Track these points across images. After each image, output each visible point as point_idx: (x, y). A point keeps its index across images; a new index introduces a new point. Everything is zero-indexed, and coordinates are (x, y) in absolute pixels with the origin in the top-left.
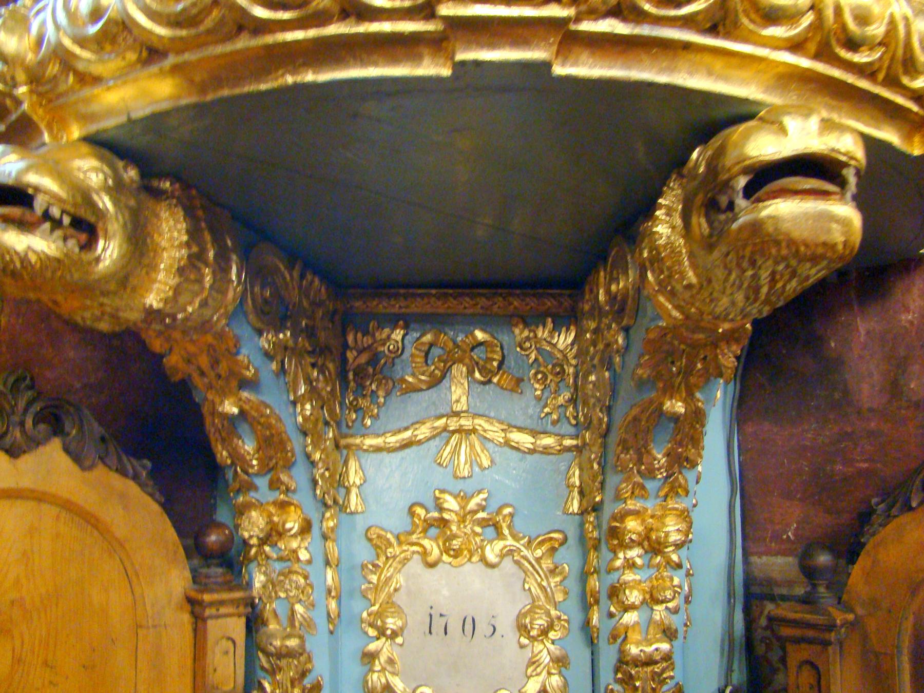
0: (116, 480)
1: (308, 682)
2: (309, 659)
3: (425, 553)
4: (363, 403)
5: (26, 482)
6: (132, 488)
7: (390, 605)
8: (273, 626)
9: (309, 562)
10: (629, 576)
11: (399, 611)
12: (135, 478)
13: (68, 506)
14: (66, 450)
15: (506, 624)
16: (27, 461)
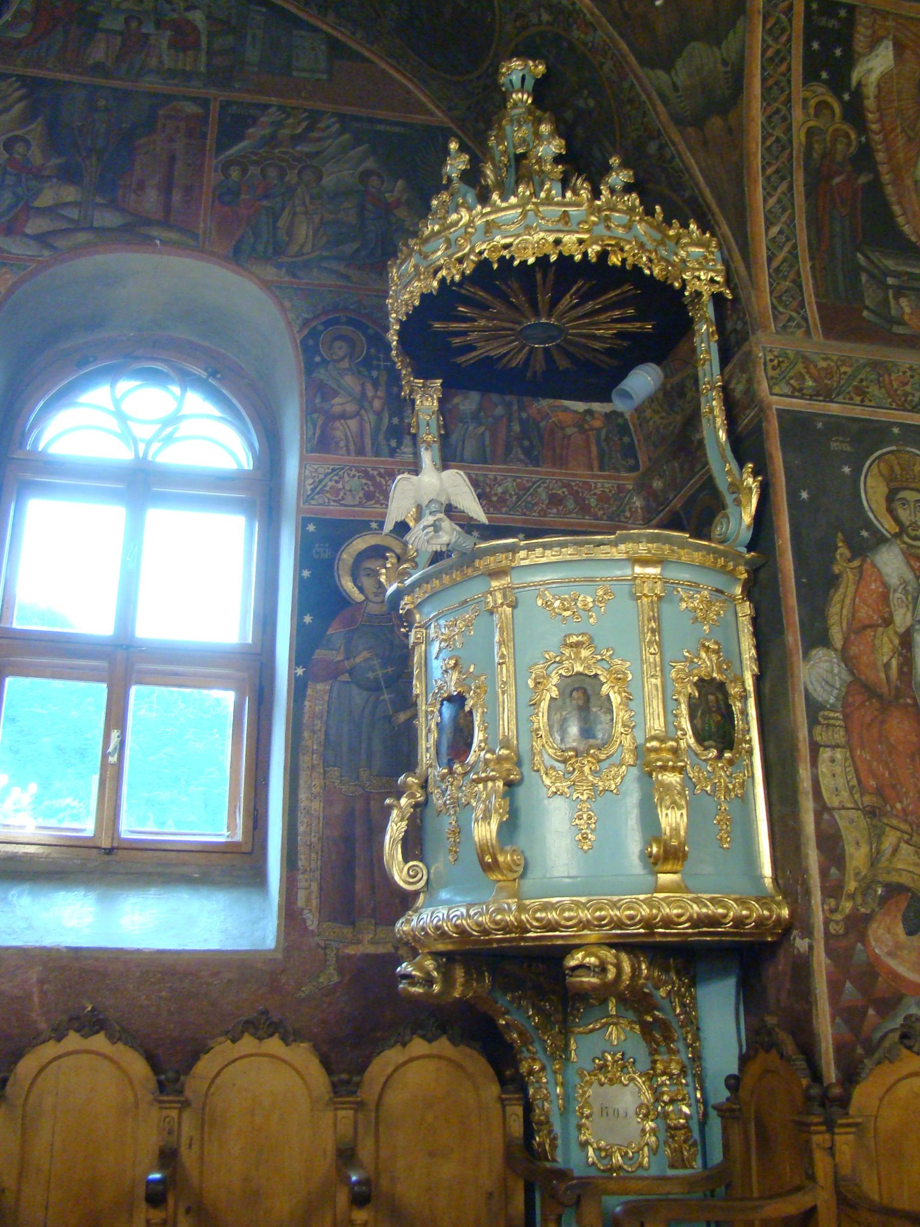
0: (468, 1050)
1: (552, 1136)
2: (551, 1126)
3: (599, 1080)
4: (575, 1012)
5: (435, 1052)
6: (475, 1054)
7: (587, 1104)
8: (537, 1111)
9: (547, 1083)
10: (665, 1089)
11: (590, 1106)
12: (475, 1049)
13: (450, 1060)
14: (449, 1040)
15: (631, 1112)
16: (435, 1044)
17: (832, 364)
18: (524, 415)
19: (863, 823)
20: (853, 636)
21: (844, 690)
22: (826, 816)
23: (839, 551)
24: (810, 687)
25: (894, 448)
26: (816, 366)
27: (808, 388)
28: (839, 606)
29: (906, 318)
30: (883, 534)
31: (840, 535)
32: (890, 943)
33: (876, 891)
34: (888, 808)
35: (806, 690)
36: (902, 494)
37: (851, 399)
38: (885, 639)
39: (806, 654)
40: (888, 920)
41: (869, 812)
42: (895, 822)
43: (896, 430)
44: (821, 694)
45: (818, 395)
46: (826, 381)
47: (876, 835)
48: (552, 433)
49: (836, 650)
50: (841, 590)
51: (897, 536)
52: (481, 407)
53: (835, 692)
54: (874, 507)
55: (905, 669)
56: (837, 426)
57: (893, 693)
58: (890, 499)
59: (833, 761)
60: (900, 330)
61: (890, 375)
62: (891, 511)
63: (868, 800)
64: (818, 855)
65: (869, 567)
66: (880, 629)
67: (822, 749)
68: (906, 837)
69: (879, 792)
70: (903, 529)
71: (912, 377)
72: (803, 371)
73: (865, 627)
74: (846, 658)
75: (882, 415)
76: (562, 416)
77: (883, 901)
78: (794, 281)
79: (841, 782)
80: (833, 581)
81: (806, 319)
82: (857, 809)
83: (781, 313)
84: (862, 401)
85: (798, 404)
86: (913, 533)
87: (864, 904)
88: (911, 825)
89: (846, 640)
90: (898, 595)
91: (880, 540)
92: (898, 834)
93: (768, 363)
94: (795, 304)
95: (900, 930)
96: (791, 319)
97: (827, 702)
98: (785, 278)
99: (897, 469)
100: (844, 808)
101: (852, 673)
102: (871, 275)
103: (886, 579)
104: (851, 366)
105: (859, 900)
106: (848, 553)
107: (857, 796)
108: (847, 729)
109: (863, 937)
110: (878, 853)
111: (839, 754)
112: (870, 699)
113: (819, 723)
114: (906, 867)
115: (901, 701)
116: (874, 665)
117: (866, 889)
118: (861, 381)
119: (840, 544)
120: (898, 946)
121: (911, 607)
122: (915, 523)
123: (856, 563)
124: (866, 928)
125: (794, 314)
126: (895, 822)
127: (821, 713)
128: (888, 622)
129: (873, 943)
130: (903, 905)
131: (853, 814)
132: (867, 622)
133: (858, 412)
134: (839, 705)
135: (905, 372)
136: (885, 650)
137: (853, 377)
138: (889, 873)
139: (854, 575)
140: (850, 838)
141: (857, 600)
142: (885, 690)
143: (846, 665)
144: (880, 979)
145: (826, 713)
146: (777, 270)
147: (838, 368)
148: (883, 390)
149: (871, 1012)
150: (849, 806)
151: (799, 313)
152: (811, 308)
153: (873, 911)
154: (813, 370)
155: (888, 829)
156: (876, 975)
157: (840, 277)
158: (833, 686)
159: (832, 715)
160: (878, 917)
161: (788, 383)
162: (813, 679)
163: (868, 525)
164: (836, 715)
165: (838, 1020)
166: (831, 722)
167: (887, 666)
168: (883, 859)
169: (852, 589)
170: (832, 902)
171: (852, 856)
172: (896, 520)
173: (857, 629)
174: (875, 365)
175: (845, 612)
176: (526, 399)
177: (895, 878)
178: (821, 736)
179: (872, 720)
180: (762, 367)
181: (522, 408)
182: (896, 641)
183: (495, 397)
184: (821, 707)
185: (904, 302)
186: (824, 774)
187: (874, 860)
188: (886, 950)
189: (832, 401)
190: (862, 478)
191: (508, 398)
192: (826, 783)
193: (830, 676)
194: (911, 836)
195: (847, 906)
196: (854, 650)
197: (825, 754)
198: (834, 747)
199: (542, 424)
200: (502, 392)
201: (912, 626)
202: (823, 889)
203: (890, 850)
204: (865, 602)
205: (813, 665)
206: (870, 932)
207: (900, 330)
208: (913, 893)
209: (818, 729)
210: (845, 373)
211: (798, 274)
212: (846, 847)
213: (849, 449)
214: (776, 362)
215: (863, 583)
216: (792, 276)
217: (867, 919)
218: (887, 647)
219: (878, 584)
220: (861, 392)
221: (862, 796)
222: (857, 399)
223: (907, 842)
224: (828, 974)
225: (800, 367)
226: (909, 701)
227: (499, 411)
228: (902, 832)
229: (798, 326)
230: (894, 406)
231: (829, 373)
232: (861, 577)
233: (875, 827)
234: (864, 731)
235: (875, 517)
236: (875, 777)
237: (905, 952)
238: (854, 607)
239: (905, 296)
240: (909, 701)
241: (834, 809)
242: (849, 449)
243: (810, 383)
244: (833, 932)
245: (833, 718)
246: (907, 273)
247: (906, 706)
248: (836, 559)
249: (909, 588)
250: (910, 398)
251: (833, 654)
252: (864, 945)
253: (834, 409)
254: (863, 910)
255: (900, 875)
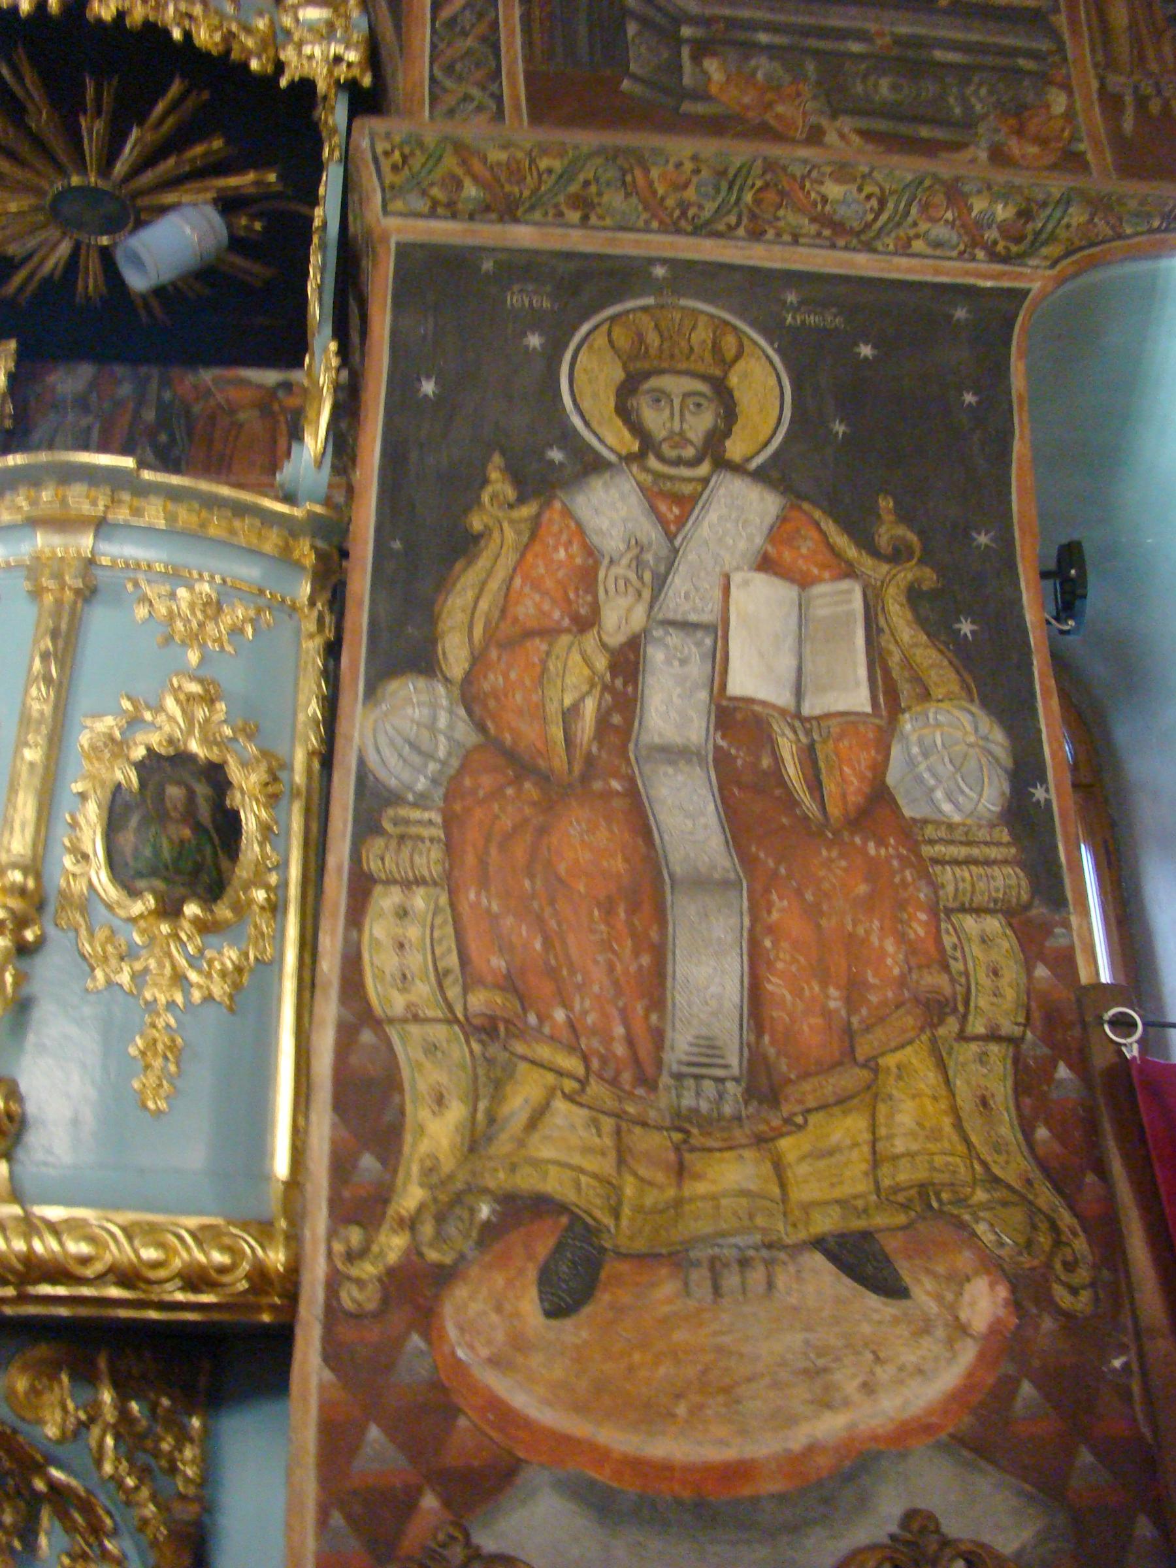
17: (520, 155)
18: (167, 396)
19: (459, 1050)
20: (494, 654)
21: (455, 763)
22: (367, 1036)
23: (489, 489)
24: (372, 759)
25: (650, 301)
26: (484, 159)
27: (468, 199)
28: (470, 595)
29: (714, 89)
30: (597, 456)
31: (497, 459)
32: (500, 1336)
33: (473, 1211)
34: (532, 1019)
35: (361, 762)
36: (654, 382)
37: (560, 214)
38: (575, 657)
39: (371, 691)
40: (499, 1280)
41: (479, 1029)
42: (544, 1052)
43: (660, 271)
44: (393, 769)
45: (488, 209)
46: (508, 188)
47: (491, 1082)
48: (212, 419)
49: (447, 680)
50: (483, 562)
51: (638, 458)
52: (93, 385)
53: (432, 767)
54: (585, 405)
55: (616, 719)
56: (523, 267)
57: (577, 769)
58: (627, 390)
59: (403, 913)
60: (700, 108)
61: (647, 171)
62: (624, 411)
63: (479, 1001)
64: (334, 1126)
65: (556, 516)
66: (565, 639)
67: (378, 889)
68: (569, 1085)
69: (510, 984)
70: (648, 444)
71: (697, 171)
72: (459, 172)
73: (529, 634)
74: (470, 696)
75: (629, 245)
76: (233, 394)
77: (489, 1233)
78: (483, 39)
79: (415, 960)
80: (464, 545)
81: (499, 99)
82: (452, 1020)
83: (445, 90)
84: (585, 218)
85: (445, 231)
86: (672, 454)
87: (440, 1237)
88: (585, 1059)
89: (478, 660)
90: (619, 570)
91: (591, 465)
92: (550, 1078)
93: (382, 159)
94: (479, 75)
95: (529, 1305)
96: (467, 98)
97: (410, 788)
98: (465, 34)
99: (653, 339)
100: (416, 1018)
101: (481, 728)
102: (644, 21)
103: (595, 539)
104: (561, 155)
105: (427, 1229)
106: (511, 493)
107: (453, 992)
108: (450, 848)
109: (426, 1319)
110: (491, 1120)
111: (419, 901)
112: (517, 781)
113: (379, 831)
114: (563, 1157)
115: (597, 785)
116: (539, 713)
117: (449, 1204)
118: (587, 184)
119: (494, 475)
120: (519, 1343)
121: (647, 594)
122: (682, 433)
123: (527, 511)
124: (437, 1298)
125: (475, 92)
126: (544, 1052)
127: (391, 812)
128: (586, 622)
129: (452, 1332)
130: (543, 1248)
131: (439, 1033)
132: (533, 624)
133: (579, 240)
134: (438, 794)
135: (679, 165)
136: (571, 680)
137: (566, 176)
138: (513, 1168)
139: (519, 533)
140: (422, 1086)
141: (518, 582)
142: (559, 761)
143: (469, 712)
144: (462, 1422)
145: (403, 812)
146: (452, 22)
147: (532, 161)
148: (634, 200)
149: (429, 1502)
150: (430, 1013)
151: (484, 89)
152: (513, 84)
153: (462, 1257)
154: (477, 166)
155: (523, 1067)
156: (451, 1412)
157: (583, 30)
158: (429, 756)
159: (416, 814)
160: (474, 1271)
161: (424, 193)
162: (383, 741)
163: (568, 438)
164: (426, 815)
165: (337, 1519)
166: (413, 830)
167: (570, 715)
168: (504, 1136)
169: (508, 559)
170: (355, 1235)
171: (421, 1130)
172: (637, 428)
173: (506, 637)
174: (612, 155)
175: (484, 605)
176: (175, 372)
177: (527, 1181)
178: (380, 857)
179: (517, 829)
180: (372, 168)
181: (165, 383)
182: (601, 663)
183: (120, 370)
184: (394, 798)
185: (712, 66)
186: (376, 943)
187: (476, 1141)
188: (485, 1352)
189: (516, 220)
190: (568, 357)
191: (143, 370)
192: (380, 963)
193: (426, 734)
194: (583, 1083)
195: (393, 1245)
196: (493, 680)
197: (385, 900)
198: (408, 884)
199: (196, 409)
200: (134, 360)
201: (646, 631)
202: (335, 1202)
203: (523, 1118)
204: (536, 585)
205: (386, 714)
206: (448, 1310)
207: (700, 108)
208: (575, 1218)
209: (377, 845)
210: (550, 171)
211: (494, 26)
212: (409, 1108)
213: (546, 304)
214: (397, 154)
215: (537, 547)
216: (482, 28)
217: (444, 1276)
218: (573, 678)
219: (575, 548)
220: (585, 205)
221: (466, 990)
222: (574, 216)
223: (569, 1098)
224: (325, 1406)
225: (450, 162)
226: (616, 785)
227: (125, 390)
228: (560, 1073)
229: (480, 109)
230: (655, 225)
231: (515, 172)
232: (533, 536)
233: (490, 1062)
234: (493, 851)
235: (587, 424)
236: (504, 947)
237: (536, 1361)
238: (507, 595)
239: (714, 54)
240: (616, 785)
241: (391, 1021)
242: (546, 304)
243: (471, 190)
244: (347, 1304)
245: (419, 822)
246: (726, 19)
247: (609, 794)
248: (478, 500)
249: (649, 557)
250: (691, 213)
251: (441, 690)
252: (426, 1337)
253: (523, 235)
254: (433, 1255)
255: (545, 1176)
